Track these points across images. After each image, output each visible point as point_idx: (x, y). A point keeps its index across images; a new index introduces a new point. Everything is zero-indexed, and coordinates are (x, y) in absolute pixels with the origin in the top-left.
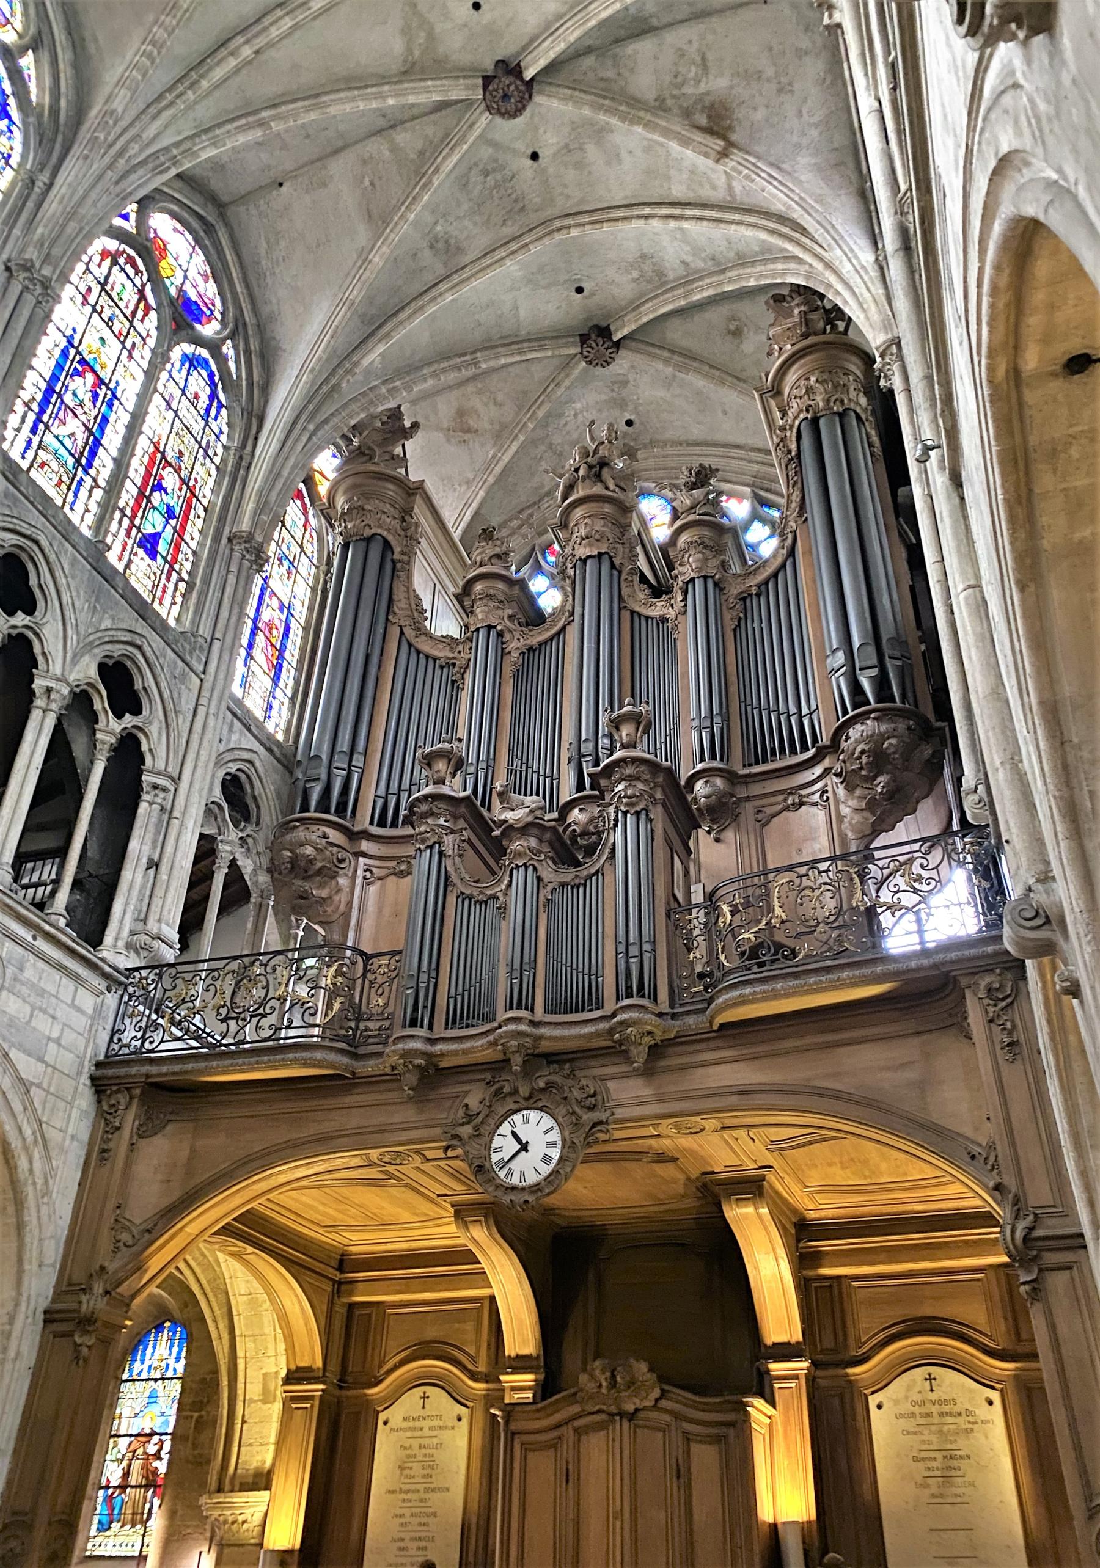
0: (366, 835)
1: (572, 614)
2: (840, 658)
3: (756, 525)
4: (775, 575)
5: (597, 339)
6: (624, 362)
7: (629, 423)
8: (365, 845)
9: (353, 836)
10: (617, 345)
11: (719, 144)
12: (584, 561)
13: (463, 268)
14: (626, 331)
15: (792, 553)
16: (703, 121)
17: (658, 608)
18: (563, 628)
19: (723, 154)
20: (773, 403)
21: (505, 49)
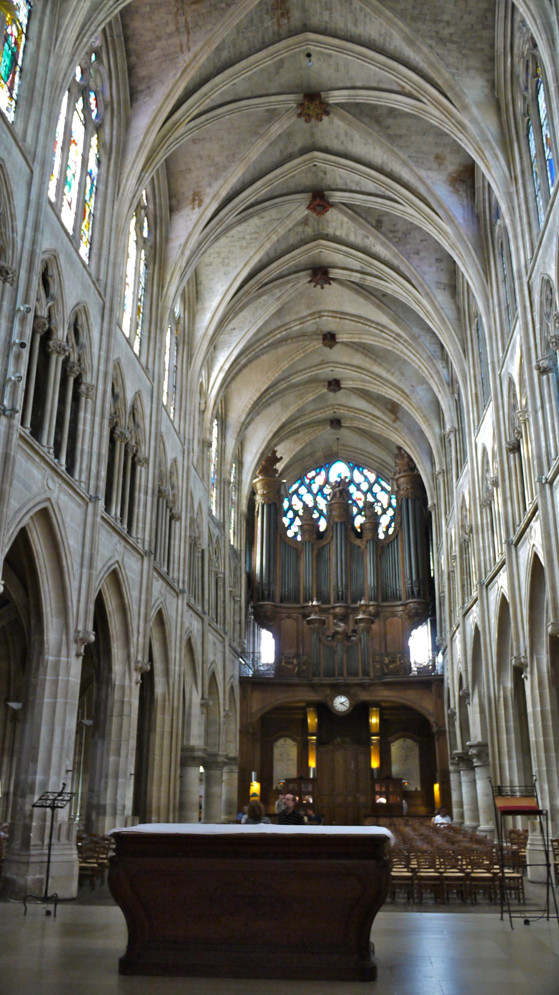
0: (280, 607)
1: (332, 538)
2: (409, 582)
3: (376, 485)
4: (391, 542)
5: (336, 423)
6: (342, 429)
7: (338, 439)
8: (278, 610)
9: (276, 607)
10: (342, 427)
11: (393, 417)
12: (337, 523)
13: (305, 415)
14: (346, 425)
15: (397, 536)
16: (390, 407)
17: (358, 542)
18: (329, 543)
19: (394, 421)
20: (394, 482)
21: (337, 377)
